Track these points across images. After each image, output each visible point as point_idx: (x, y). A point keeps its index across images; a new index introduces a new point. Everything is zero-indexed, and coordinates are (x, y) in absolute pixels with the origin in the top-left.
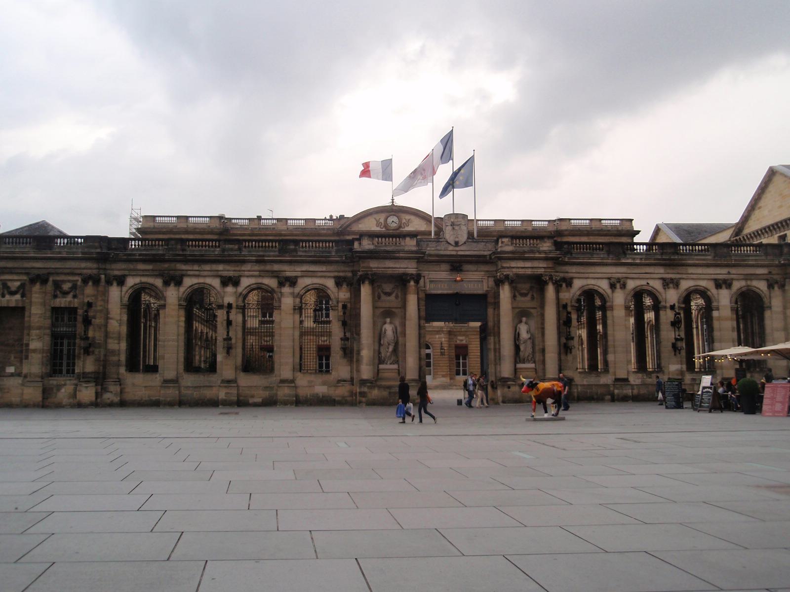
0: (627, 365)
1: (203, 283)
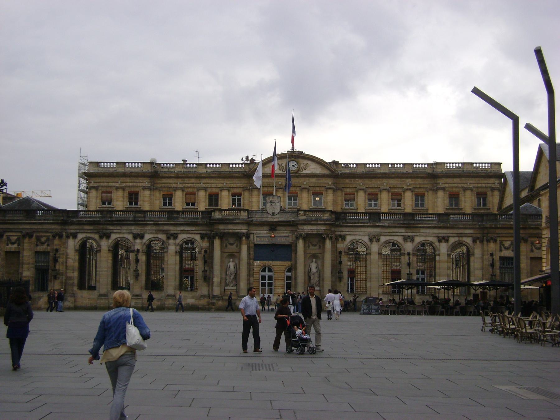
0: (379, 289)
1: (122, 237)
